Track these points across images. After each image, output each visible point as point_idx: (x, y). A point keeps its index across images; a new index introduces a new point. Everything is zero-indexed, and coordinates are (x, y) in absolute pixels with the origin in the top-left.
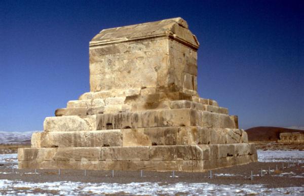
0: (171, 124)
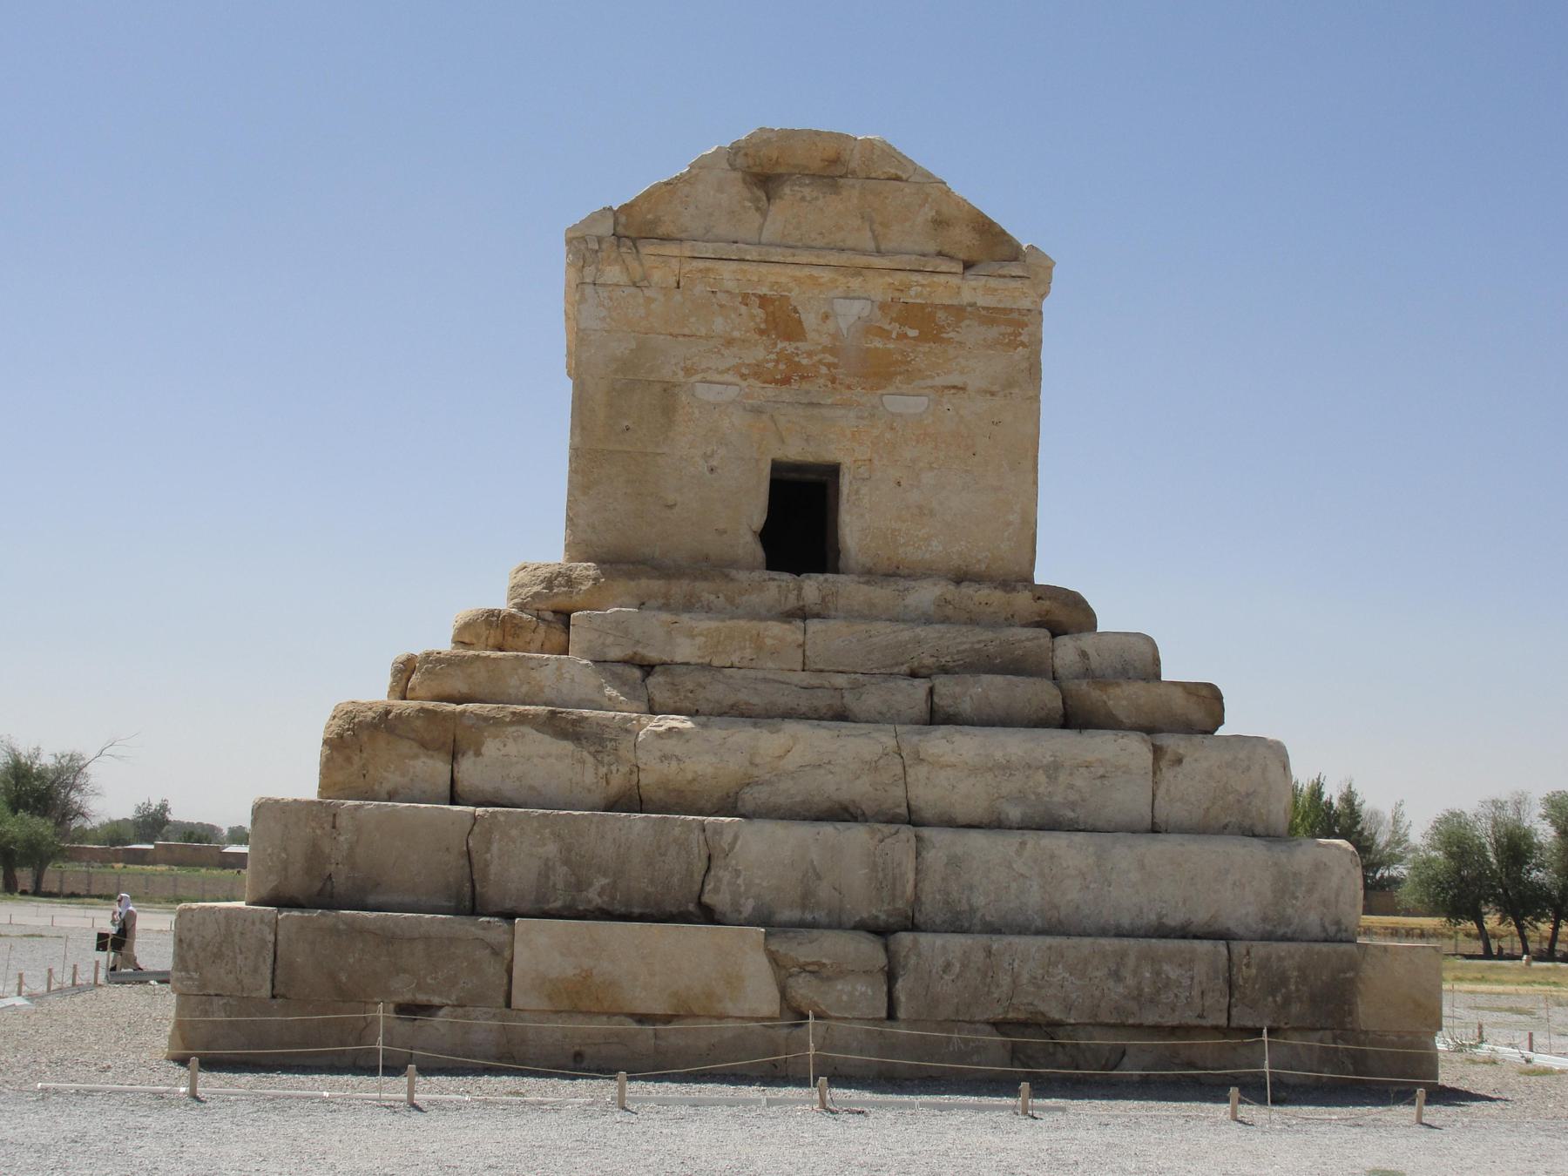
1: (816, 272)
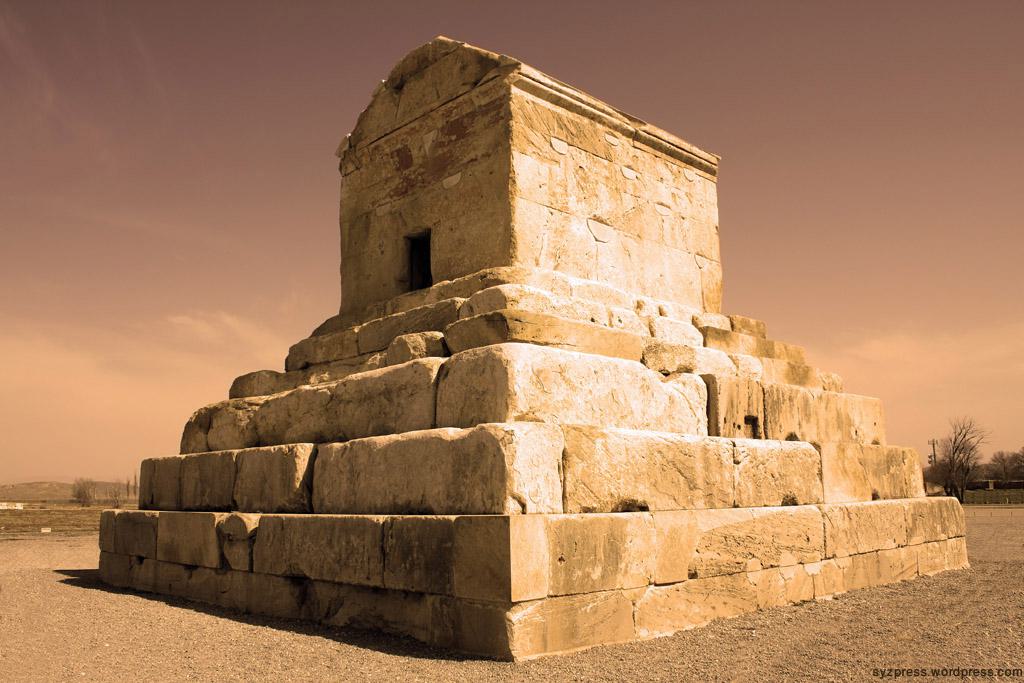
1: (412, 125)
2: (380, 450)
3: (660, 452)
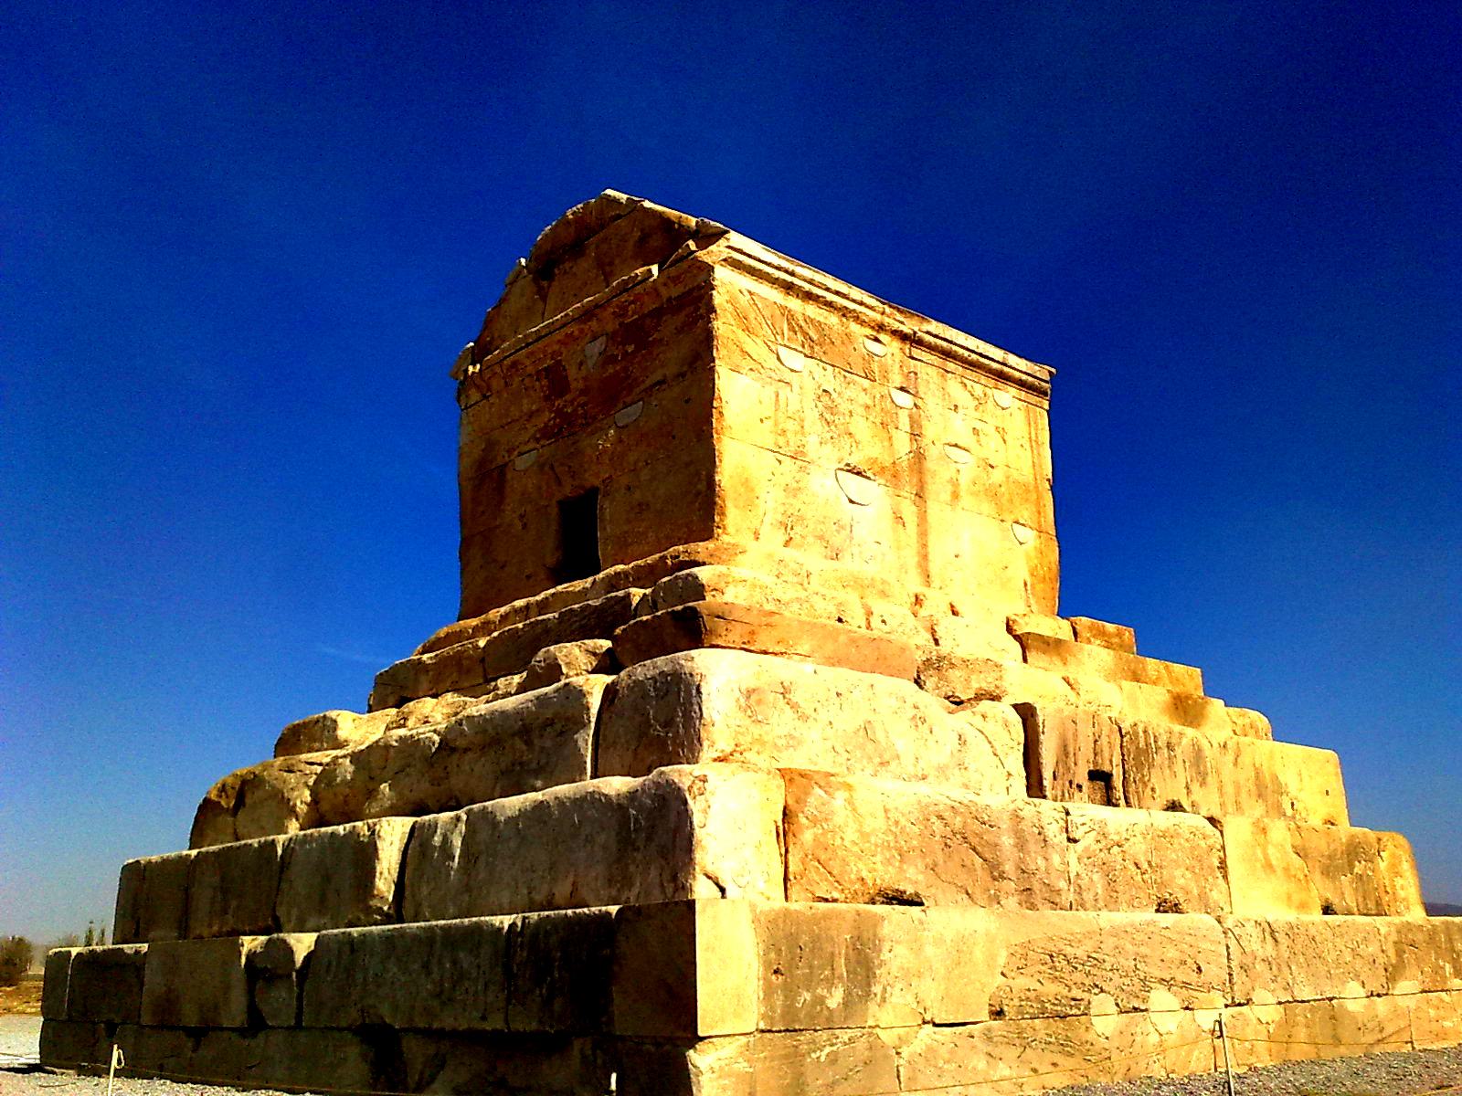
0: (1303, 815)
2: (510, 820)
3: (940, 817)
